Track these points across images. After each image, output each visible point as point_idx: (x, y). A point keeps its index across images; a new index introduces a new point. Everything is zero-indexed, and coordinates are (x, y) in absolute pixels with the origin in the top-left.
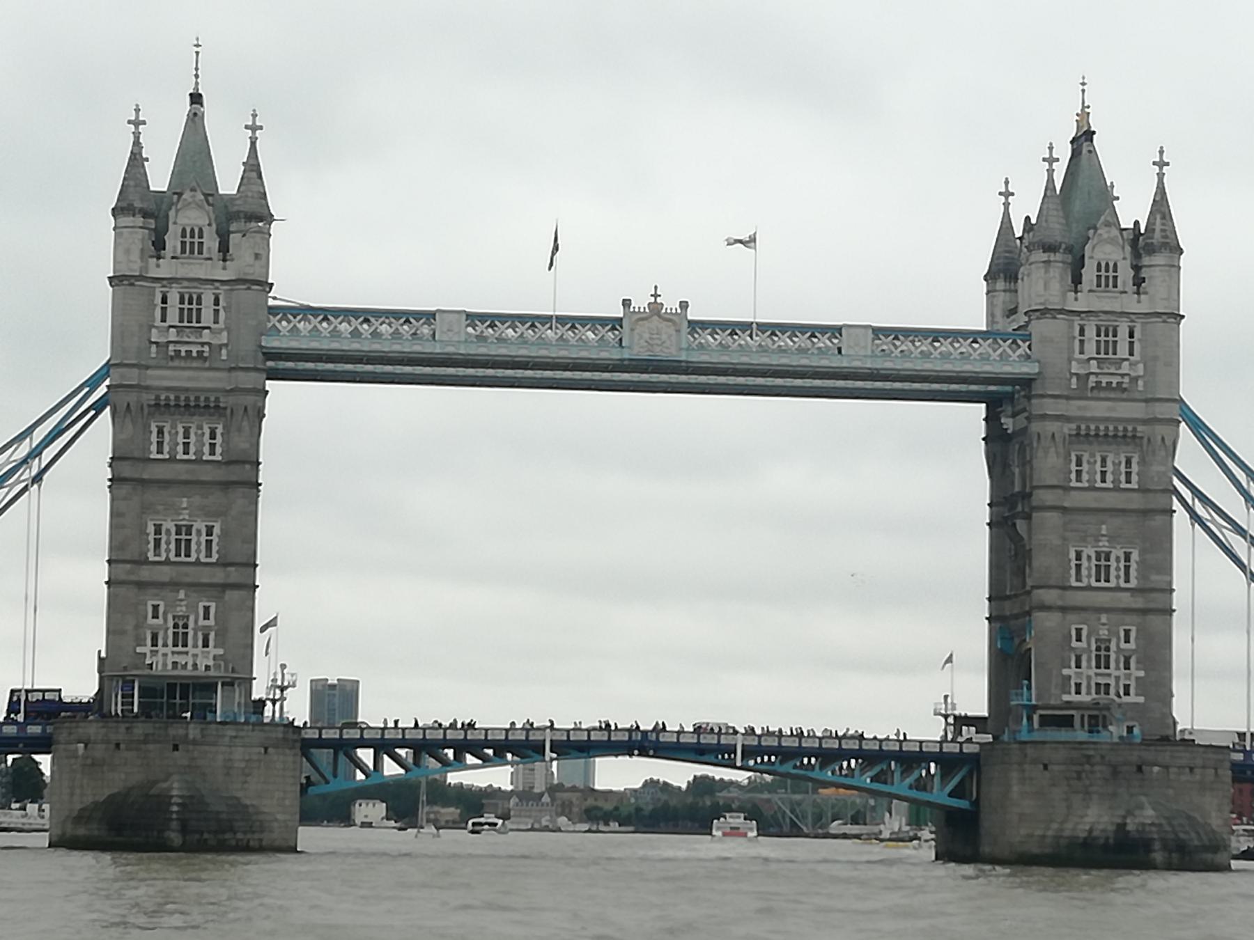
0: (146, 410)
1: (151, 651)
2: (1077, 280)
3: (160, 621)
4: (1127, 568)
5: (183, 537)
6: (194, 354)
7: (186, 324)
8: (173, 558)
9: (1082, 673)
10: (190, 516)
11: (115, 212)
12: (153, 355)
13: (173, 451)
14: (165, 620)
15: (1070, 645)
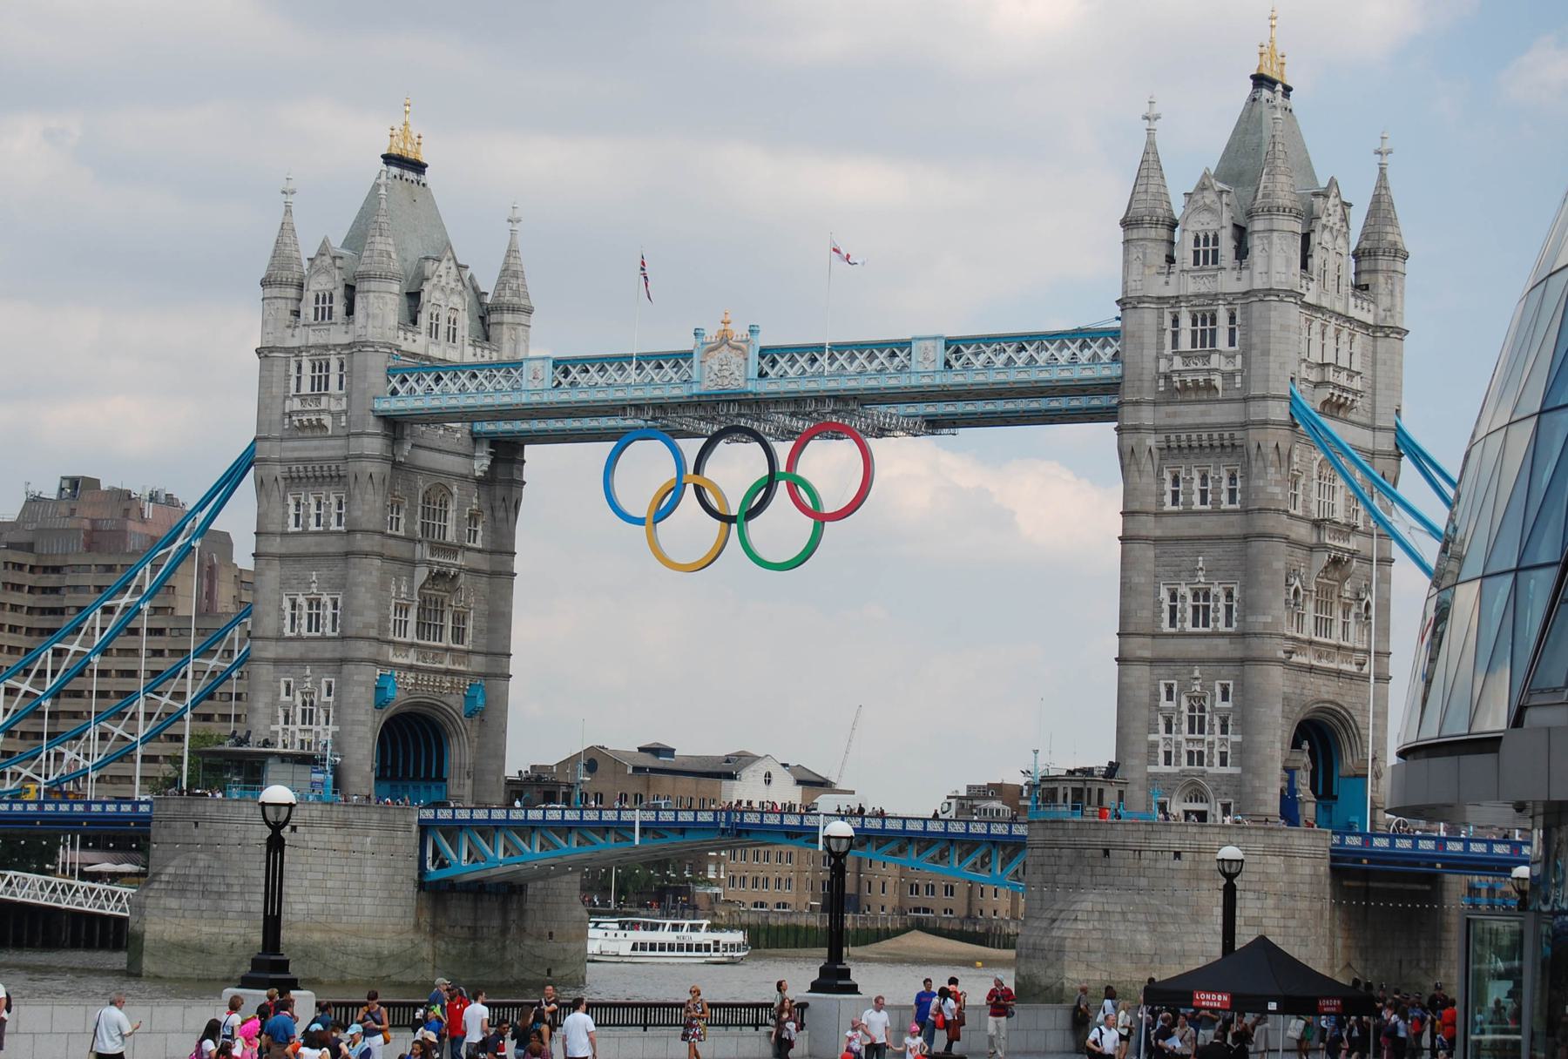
0: (282, 484)
1: (284, 729)
2: (1170, 260)
3: (290, 699)
4: (1229, 609)
5: (314, 611)
6: (314, 423)
7: (316, 392)
8: (304, 632)
9: (1171, 739)
10: (318, 588)
11: (265, 283)
12: (287, 427)
13: (306, 523)
14: (294, 696)
15: (1158, 706)
